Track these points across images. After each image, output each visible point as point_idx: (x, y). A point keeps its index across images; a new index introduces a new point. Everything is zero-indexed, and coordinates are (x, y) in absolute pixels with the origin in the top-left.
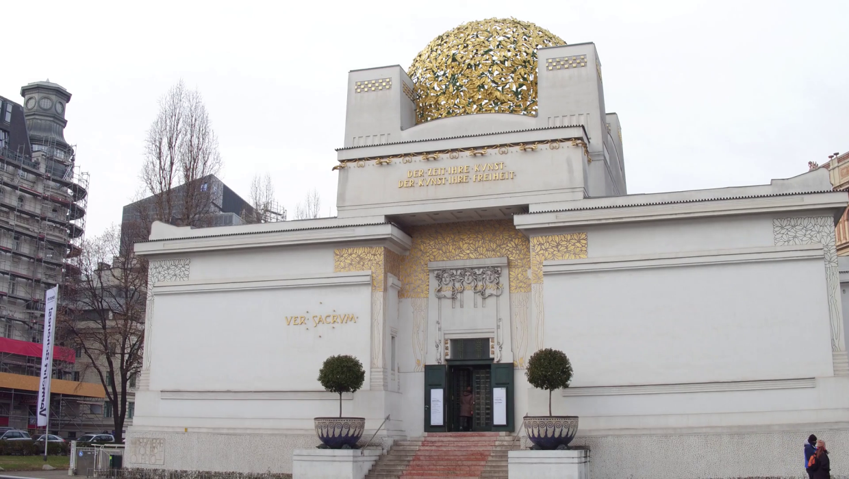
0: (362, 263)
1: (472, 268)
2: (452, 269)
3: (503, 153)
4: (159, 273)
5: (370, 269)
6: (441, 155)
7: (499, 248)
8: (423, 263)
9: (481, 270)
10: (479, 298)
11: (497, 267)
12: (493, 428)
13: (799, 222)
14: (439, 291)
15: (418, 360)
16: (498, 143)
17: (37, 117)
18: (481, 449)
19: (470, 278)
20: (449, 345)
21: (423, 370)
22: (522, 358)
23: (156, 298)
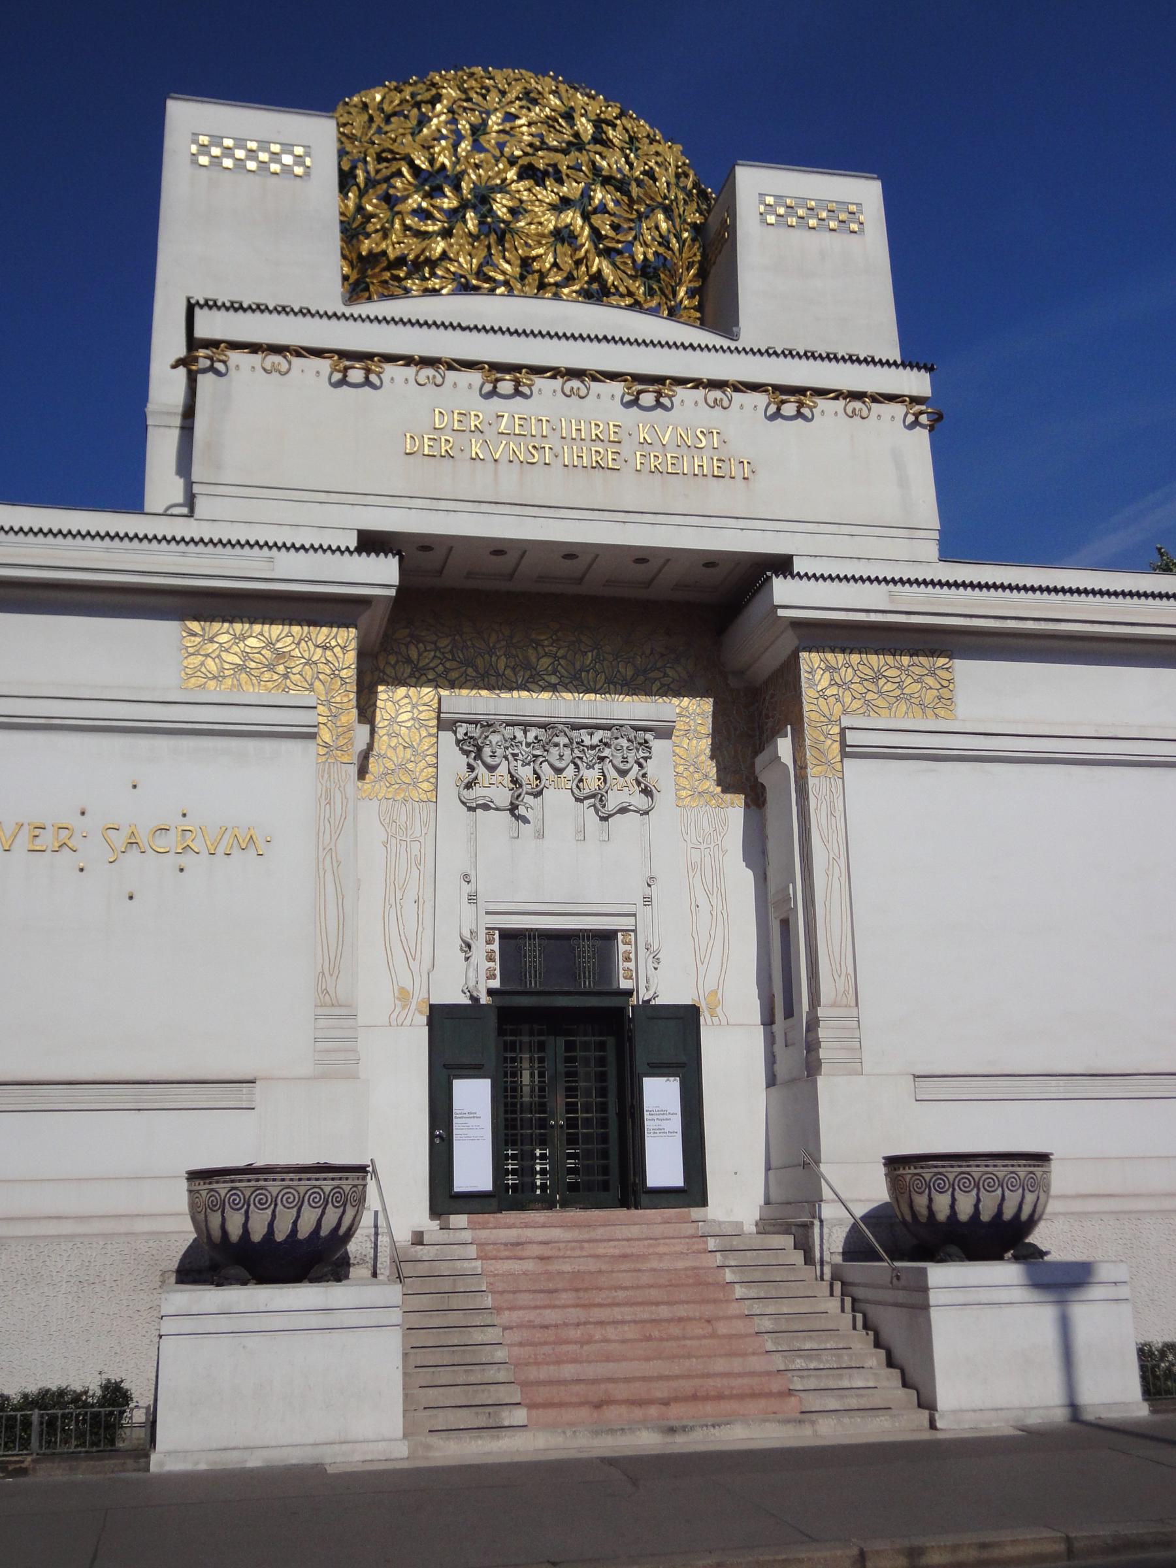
0: (281, 669)
1: (575, 727)
2: (513, 725)
5: (311, 688)
7: (641, 678)
8: (414, 701)
9: (599, 735)
11: (646, 729)
12: (644, 1199)
15: (402, 990)
16: (706, 374)
18: (680, 1265)
19: (567, 752)
20: (496, 946)
21: (423, 1020)
22: (715, 992)
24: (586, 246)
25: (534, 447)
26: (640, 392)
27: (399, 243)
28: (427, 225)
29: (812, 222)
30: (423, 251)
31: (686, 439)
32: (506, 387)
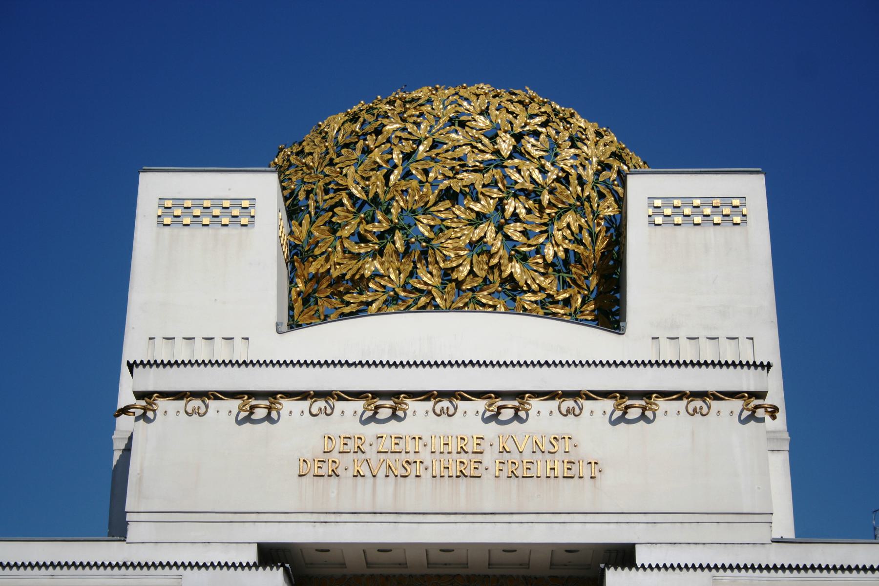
24: (501, 252)
25: (407, 462)
26: (500, 408)
27: (339, 264)
28: (360, 248)
29: (698, 219)
30: (359, 269)
31: (541, 448)
32: (384, 413)
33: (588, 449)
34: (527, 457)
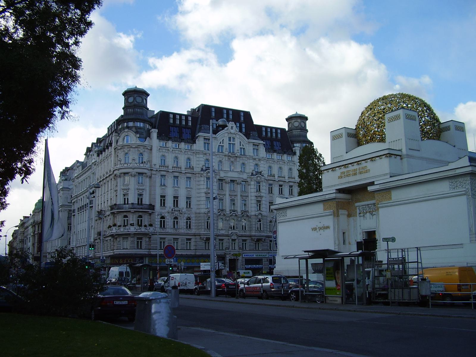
1: (368, 205)
3: (366, 162)
4: (279, 215)
6: (349, 165)
10: (371, 216)
13: (458, 180)
14: (360, 213)
17: (293, 131)
23: (279, 224)
33: (368, 168)
34: (362, 170)
